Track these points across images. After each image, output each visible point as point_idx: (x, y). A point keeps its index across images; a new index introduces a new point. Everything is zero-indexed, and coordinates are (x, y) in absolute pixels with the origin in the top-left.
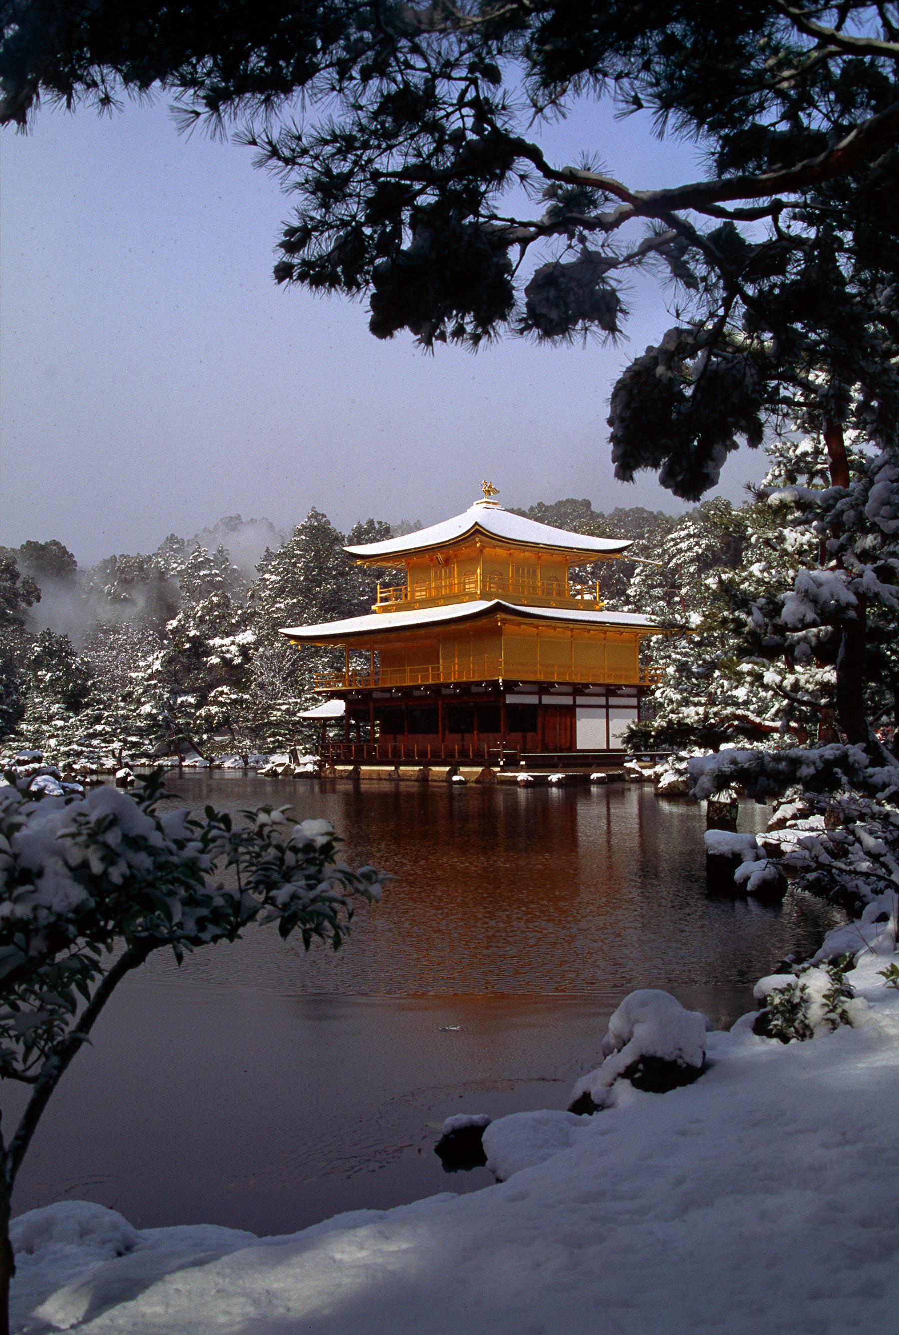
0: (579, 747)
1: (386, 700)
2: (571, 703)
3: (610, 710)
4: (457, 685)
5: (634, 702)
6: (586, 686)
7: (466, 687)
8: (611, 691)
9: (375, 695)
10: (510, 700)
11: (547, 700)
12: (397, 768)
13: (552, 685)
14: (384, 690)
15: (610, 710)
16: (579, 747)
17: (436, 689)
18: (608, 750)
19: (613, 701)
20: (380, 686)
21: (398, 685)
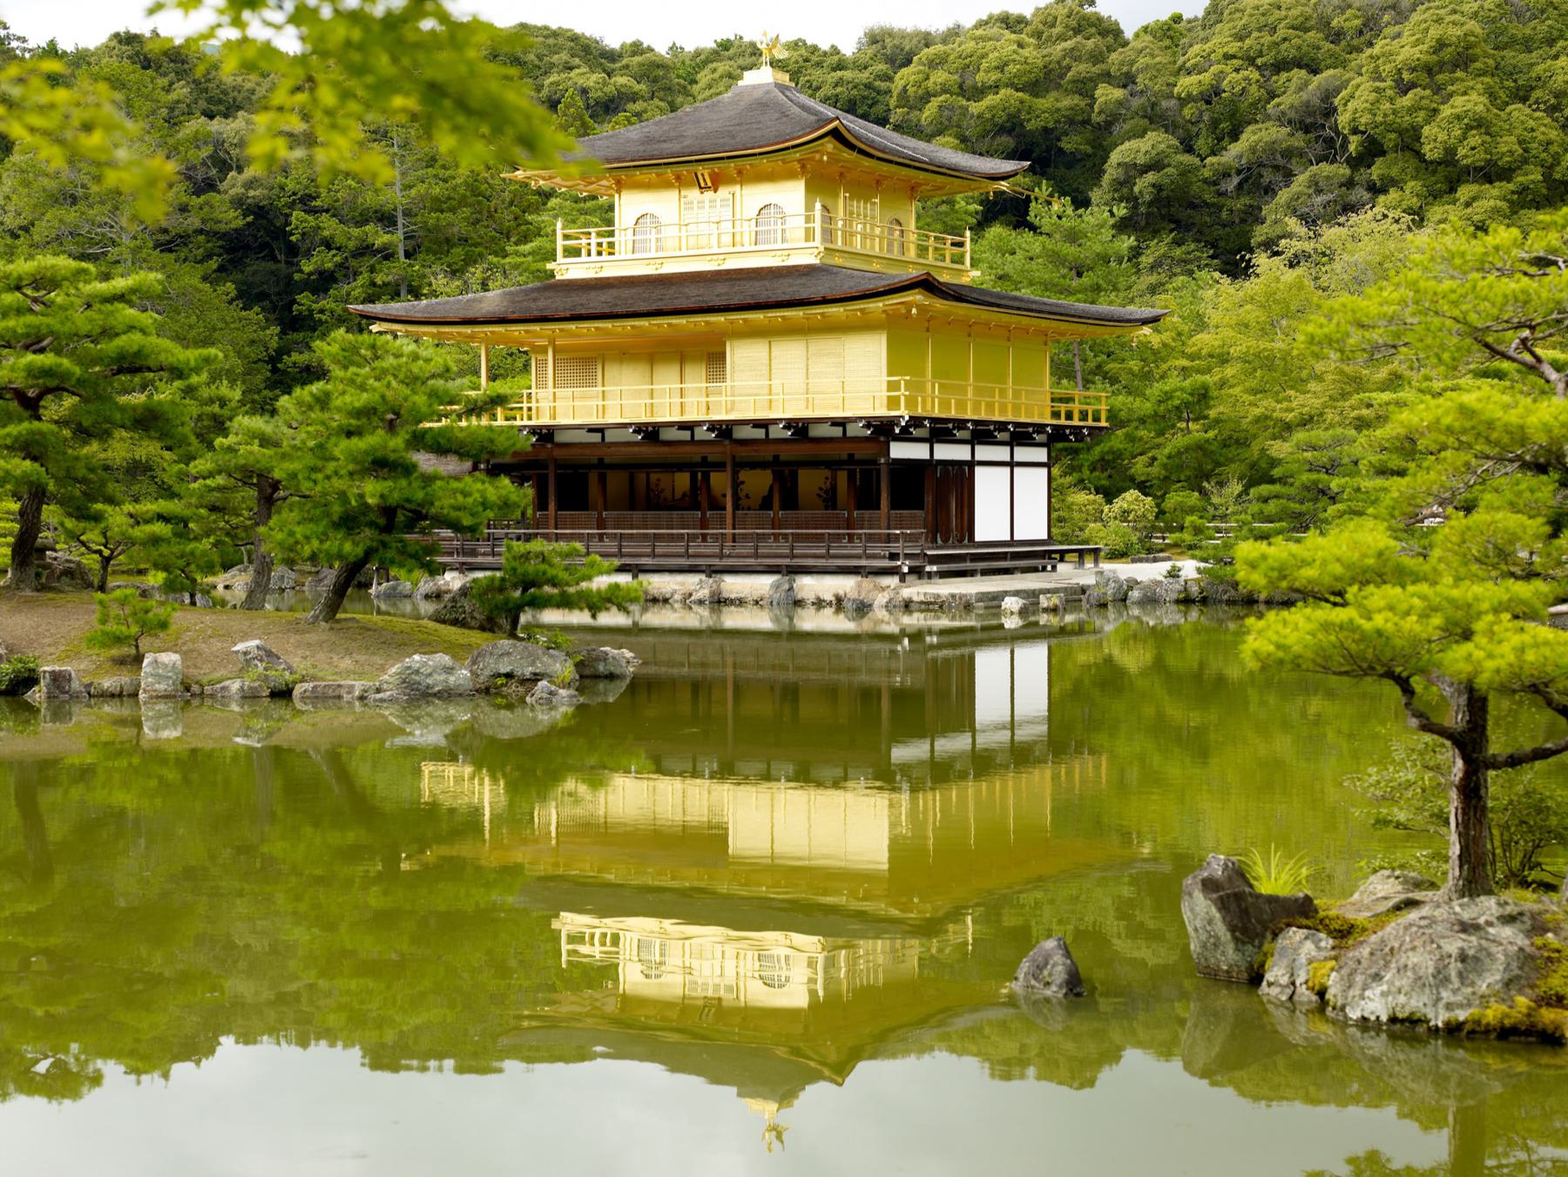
1: (594, 445)
2: (968, 458)
3: (1016, 470)
4: (790, 424)
5: (1040, 455)
6: (1002, 426)
7: (800, 427)
8: (1021, 435)
9: (560, 438)
10: (899, 451)
11: (944, 452)
12: (635, 577)
13: (961, 424)
14: (592, 429)
15: (1016, 470)
16: (977, 539)
17: (724, 430)
18: (1012, 542)
19: (1022, 454)
21: (644, 419)
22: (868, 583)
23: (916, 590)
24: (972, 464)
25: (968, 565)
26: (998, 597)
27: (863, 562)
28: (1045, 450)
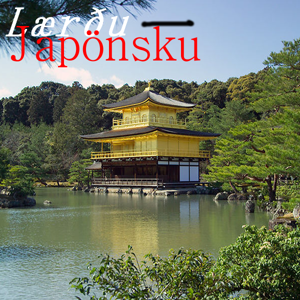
0: (181, 180)
1: (116, 162)
5: (197, 164)
6: (183, 158)
7: (145, 159)
9: (113, 160)
11: (171, 163)
14: (116, 159)
16: (181, 180)
17: (134, 159)
19: (191, 163)
20: (115, 157)
22: (152, 190)
23: (157, 192)
24: (179, 165)
25: (174, 186)
26: (165, 192)
27: (151, 185)
28: (198, 163)
